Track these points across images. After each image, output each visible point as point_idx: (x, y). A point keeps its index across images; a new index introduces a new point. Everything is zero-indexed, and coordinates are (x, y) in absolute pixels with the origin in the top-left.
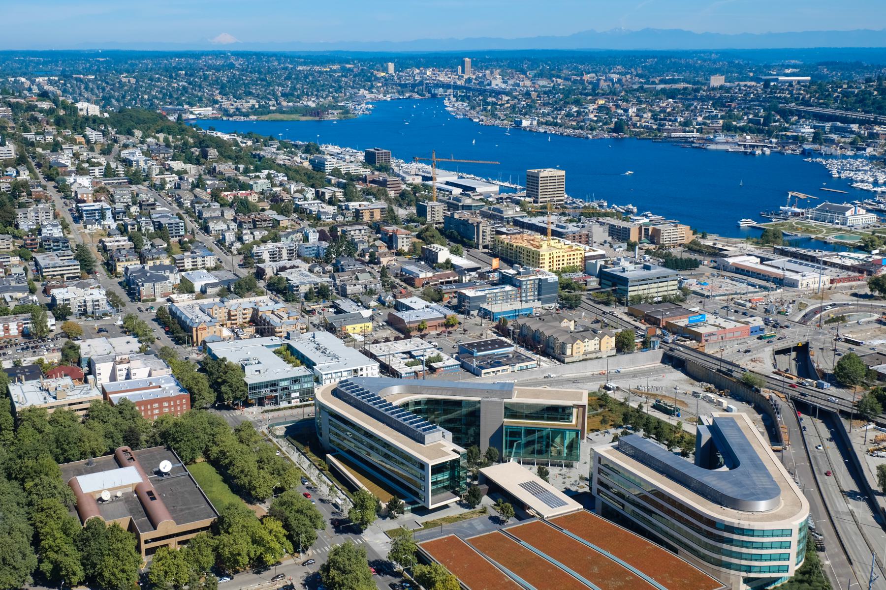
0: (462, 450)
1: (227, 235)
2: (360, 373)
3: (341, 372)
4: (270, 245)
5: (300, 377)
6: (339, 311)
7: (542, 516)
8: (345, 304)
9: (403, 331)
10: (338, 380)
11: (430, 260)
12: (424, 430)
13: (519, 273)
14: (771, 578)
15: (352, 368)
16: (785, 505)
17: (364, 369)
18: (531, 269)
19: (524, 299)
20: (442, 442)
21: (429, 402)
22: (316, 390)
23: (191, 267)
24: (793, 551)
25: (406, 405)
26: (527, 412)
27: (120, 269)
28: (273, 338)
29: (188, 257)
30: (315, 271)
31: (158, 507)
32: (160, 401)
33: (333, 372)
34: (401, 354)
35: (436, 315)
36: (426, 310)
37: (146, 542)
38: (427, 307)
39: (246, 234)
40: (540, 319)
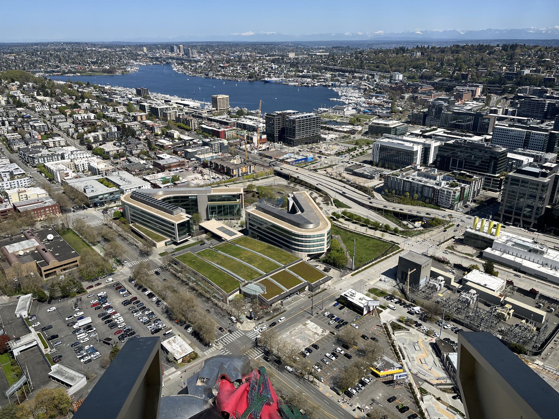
0: (190, 216)
1: (70, 130)
2: (142, 188)
4: (93, 134)
6: (130, 162)
8: (132, 159)
9: (162, 169)
11: (170, 136)
12: (173, 209)
17: (144, 186)
18: (216, 138)
20: (181, 214)
21: (174, 197)
22: (121, 197)
23: (53, 146)
24: (326, 242)
26: (217, 198)
27: (15, 148)
28: (99, 176)
31: (48, 255)
32: (44, 208)
35: (175, 160)
37: (45, 271)
38: (171, 158)
39: (80, 129)
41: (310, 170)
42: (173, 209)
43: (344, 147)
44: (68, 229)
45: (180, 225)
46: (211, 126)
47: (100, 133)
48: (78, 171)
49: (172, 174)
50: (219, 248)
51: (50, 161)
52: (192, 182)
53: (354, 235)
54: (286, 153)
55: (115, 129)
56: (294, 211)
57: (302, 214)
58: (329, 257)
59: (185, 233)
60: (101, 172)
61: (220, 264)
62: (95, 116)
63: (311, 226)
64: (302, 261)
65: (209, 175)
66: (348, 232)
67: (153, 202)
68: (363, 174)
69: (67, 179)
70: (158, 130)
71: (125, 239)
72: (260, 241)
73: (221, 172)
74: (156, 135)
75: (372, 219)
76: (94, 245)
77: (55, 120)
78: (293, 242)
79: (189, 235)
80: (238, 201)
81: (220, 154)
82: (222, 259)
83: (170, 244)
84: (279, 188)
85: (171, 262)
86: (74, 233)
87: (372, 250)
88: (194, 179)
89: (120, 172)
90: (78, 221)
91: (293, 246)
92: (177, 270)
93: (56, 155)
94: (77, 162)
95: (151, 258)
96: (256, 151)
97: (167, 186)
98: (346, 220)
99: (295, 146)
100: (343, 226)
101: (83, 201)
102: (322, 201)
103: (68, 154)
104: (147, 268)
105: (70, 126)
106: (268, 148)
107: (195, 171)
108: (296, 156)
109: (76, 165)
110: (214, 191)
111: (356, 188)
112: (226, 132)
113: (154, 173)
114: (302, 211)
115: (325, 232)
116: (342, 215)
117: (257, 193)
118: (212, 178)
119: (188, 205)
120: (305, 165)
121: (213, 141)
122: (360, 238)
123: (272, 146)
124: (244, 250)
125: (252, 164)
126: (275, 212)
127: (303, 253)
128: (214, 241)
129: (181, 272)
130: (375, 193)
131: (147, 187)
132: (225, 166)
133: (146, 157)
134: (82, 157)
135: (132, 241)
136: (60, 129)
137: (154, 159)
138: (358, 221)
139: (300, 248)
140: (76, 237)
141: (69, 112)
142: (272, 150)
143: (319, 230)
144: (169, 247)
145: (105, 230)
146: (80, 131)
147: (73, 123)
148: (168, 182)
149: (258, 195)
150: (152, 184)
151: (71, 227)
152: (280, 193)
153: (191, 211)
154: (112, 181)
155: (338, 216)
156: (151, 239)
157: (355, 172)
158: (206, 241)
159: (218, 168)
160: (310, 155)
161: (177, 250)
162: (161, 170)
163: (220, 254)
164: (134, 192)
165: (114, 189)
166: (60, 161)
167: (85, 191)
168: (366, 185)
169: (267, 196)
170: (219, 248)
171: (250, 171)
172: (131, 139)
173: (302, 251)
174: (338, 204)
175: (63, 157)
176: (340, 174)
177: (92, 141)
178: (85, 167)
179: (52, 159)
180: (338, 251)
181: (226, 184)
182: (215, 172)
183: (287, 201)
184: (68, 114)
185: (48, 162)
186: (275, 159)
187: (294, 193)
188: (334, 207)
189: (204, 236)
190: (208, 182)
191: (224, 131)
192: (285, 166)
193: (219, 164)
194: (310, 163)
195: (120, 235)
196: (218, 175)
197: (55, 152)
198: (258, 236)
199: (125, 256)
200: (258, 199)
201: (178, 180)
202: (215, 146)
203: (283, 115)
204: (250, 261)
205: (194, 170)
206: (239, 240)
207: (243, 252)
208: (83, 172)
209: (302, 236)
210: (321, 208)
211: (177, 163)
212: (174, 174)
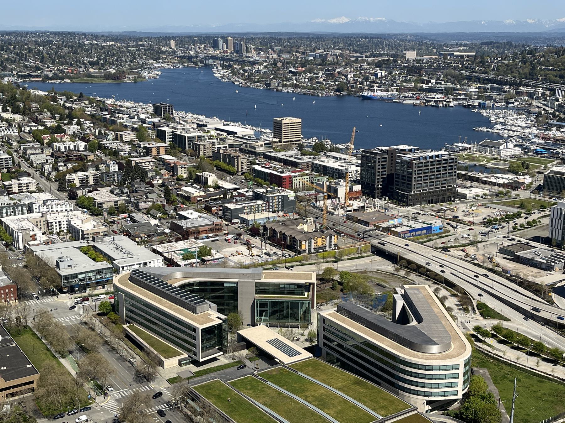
0: (223, 317)
1: (46, 166)
2: (149, 265)
3: (134, 265)
4: (80, 174)
5: (102, 269)
6: (134, 221)
7: (283, 363)
8: (138, 216)
10: (131, 271)
11: (202, 183)
12: (196, 303)
13: (267, 191)
14: (445, 400)
15: (143, 262)
16: (455, 348)
17: (152, 262)
18: (276, 188)
19: (271, 210)
20: (210, 312)
21: (200, 283)
22: (114, 278)
23: (17, 191)
24: (461, 380)
25: (183, 286)
26: (271, 289)
28: (82, 241)
29: (15, 184)
30: (115, 193)
33: (128, 265)
34: (180, 252)
35: (206, 222)
36: (199, 219)
38: (200, 217)
39: (61, 166)
40: (283, 224)
41: (437, 248)
42: (196, 303)
43: (499, 210)
44: (26, 327)
45: (206, 331)
46: (268, 168)
47: (91, 173)
48: (51, 233)
49: (200, 243)
50: (268, 376)
51: (10, 215)
52: (232, 258)
53: (513, 370)
54: (393, 217)
55: (114, 168)
56: (404, 319)
57: (419, 326)
58: (467, 409)
59: (213, 346)
60: (86, 236)
61: (269, 406)
62: (85, 146)
63: (435, 349)
64: (415, 412)
65: (261, 249)
66: (503, 365)
67: (164, 290)
68: (532, 260)
69: (35, 245)
70: (183, 172)
71: (113, 350)
72: (341, 370)
73: (281, 245)
74: (180, 179)
75: (549, 343)
76: (63, 357)
77: (25, 150)
78: (401, 375)
79: (220, 350)
80: (306, 296)
81: (281, 213)
82: (273, 397)
83: (186, 364)
84: (378, 277)
85: (186, 395)
86: (35, 334)
87: (547, 401)
88: (235, 254)
89: (117, 237)
90: (42, 314)
91: (401, 384)
92: (195, 410)
93: (20, 205)
94: (50, 218)
95: (153, 385)
96: (341, 212)
97: (190, 264)
98: (500, 342)
99: (411, 205)
100: (495, 352)
101: (54, 281)
102: (456, 305)
103: (38, 205)
104: (146, 402)
105: (47, 160)
106: (363, 207)
107: (238, 241)
108: (412, 223)
109: (48, 223)
110: (267, 276)
111: (520, 284)
112: (294, 179)
113: (171, 241)
114: (420, 320)
115: (461, 361)
116: (493, 332)
117: (340, 284)
118: (266, 254)
119: (222, 297)
120: (426, 239)
121: (271, 192)
122: (526, 377)
123: (369, 203)
124: (313, 383)
125: (334, 233)
126: (369, 319)
127: (419, 397)
128: (261, 363)
129: (201, 414)
130: (554, 296)
131: (158, 263)
132: (287, 234)
133: (160, 215)
134: (59, 209)
135: (124, 353)
136: (31, 164)
137: (172, 217)
138: (522, 345)
139: (413, 387)
140: (36, 341)
141: (47, 138)
142: (369, 210)
143: (449, 357)
144: (184, 368)
145: (84, 332)
146: (61, 168)
147: (52, 156)
148: (193, 257)
149: (341, 287)
150: (165, 259)
151: (30, 324)
152: (381, 286)
153: (225, 307)
154: (101, 252)
155: (485, 334)
156: (155, 352)
157: (518, 257)
158: (248, 363)
159: (276, 237)
160: (437, 223)
161: (198, 374)
162: (183, 237)
163: (270, 388)
164: (135, 272)
165: (104, 265)
166: (26, 216)
167: (58, 265)
168: (538, 281)
169: (356, 289)
170: (268, 376)
171: (330, 245)
172: (138, 184)
173: (416, 393)
174: (486, 312)
175: (30, 210)
176: (490, 259)
177: (78, 185)
178: (62, 226)
179: (14, 212)
180: (483, 398)
181: (287, 265)
182: (270, 244)
183: (391, 300)
184: (46, 141)
185: (7, 215)
186: (375, 225)
187: (406, 287)
188: (478, 316)
189: (245, 352)
190: (258, 260)
191: (290, 177)
192: (391, 238)
193: (278, 230)
194: (436, 237)
195: (106, 343)
196: (275, 249)
197: (20, 201)
198: (338, 360)
199: (111, 379)
200: (341, 293)
201: (209, 254)
202: (273, 200)
203: (392, 153)
204: (322, 403)
205: (237, 239)
206: (303, 365)
207: (309, 387)
208: (58, 234)
209: (417, 366)
210: (454, 318)
211: (210, 227)
212: (202, 245)
